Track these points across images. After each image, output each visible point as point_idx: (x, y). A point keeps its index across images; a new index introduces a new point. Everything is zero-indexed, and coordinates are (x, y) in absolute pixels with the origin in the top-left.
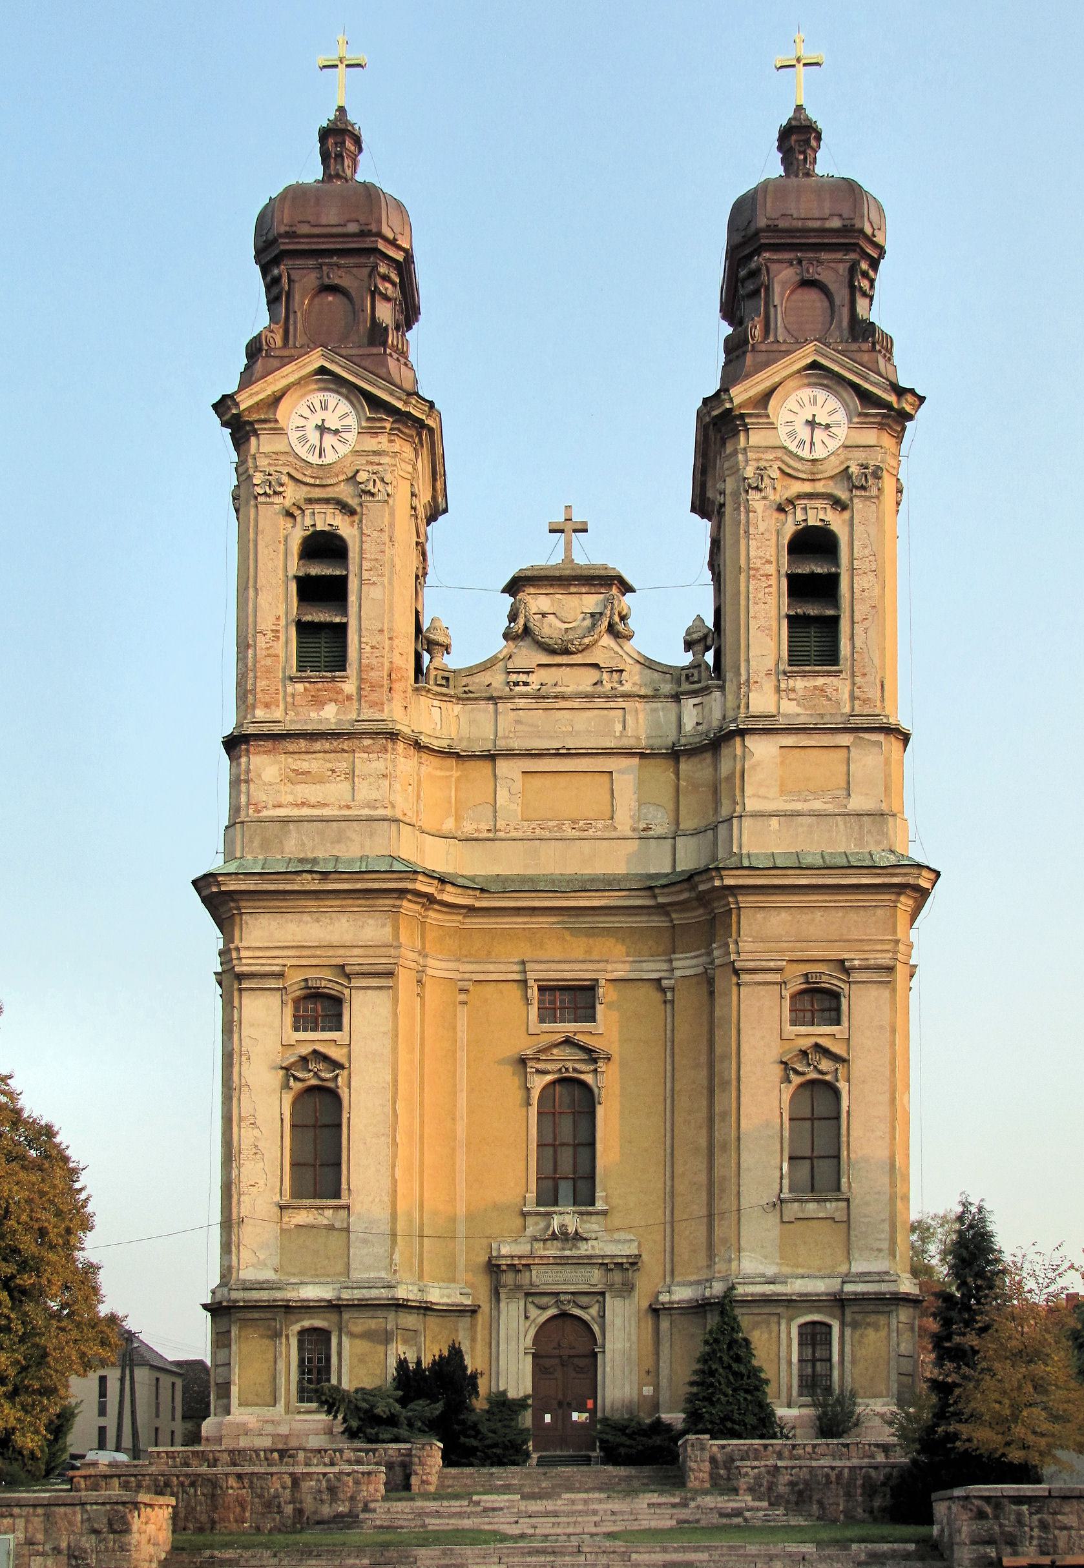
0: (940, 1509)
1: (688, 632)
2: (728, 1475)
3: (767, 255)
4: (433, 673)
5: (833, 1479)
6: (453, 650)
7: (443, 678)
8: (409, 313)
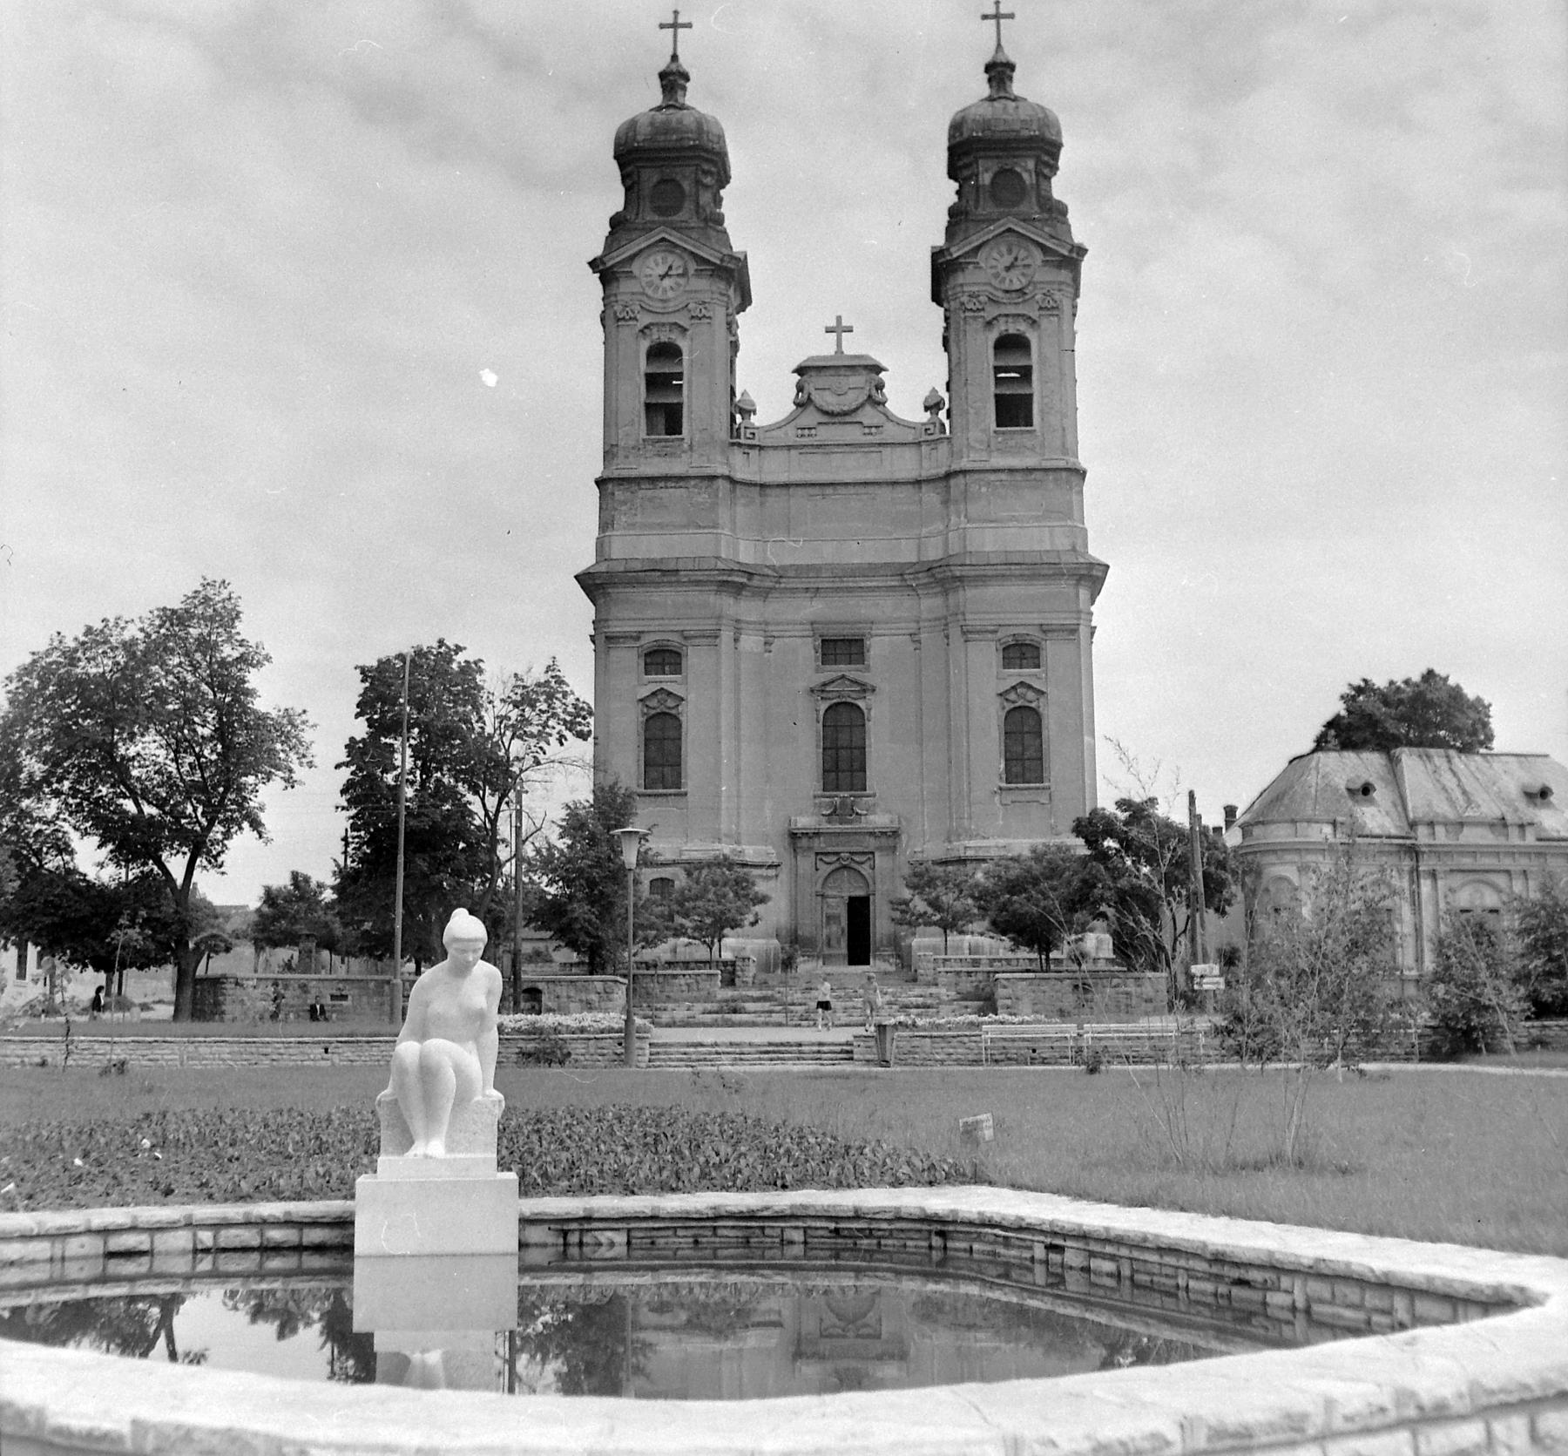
1: (926, 399)
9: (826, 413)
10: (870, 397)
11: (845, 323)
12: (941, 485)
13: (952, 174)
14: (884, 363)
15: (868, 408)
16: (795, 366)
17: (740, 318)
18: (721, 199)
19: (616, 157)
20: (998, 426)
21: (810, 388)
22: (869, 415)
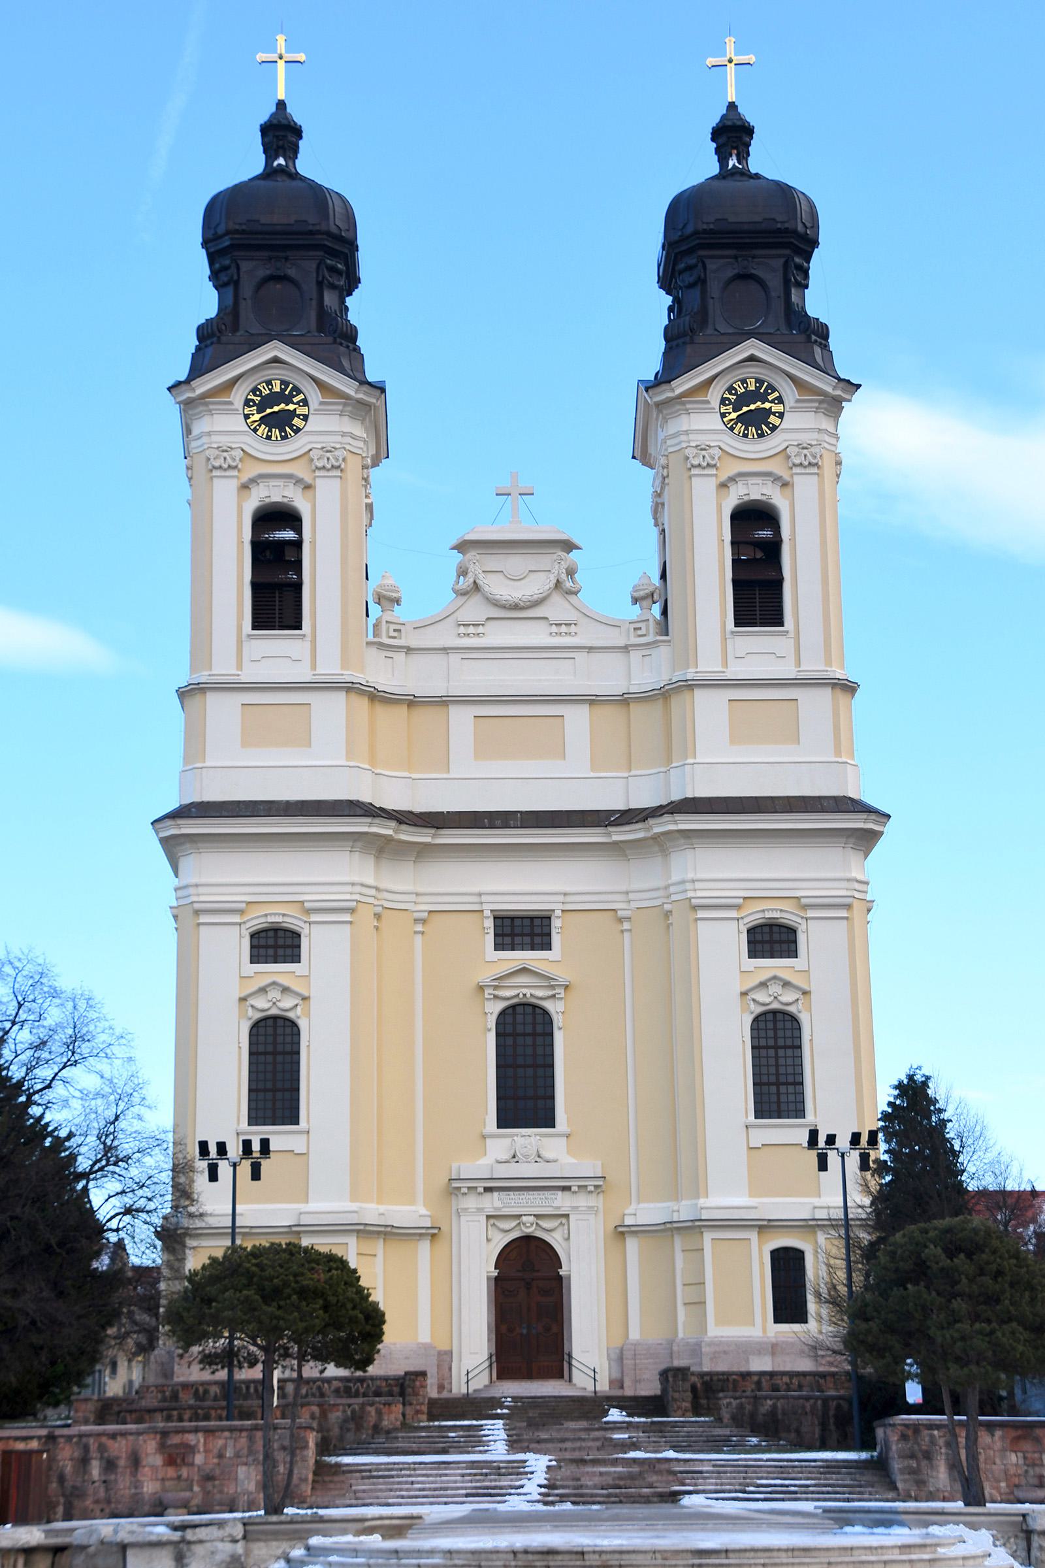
0: (880, 1433)
1: (635, 589)
2: (708, 1405)
3: (702, 253)
5: (808, 1409)
6: (403, 603)
7: (395, 630)
9: (497, 604)
10: (558, 584)
11: (524, 484)
12: (658, 706)
13: (667, 282)
14: (576, 540)
15: (557, 598)
16: (454, 541)
18: (347, 308)
19: (206, 243)
21: (475, 570)
22: (557, 609)
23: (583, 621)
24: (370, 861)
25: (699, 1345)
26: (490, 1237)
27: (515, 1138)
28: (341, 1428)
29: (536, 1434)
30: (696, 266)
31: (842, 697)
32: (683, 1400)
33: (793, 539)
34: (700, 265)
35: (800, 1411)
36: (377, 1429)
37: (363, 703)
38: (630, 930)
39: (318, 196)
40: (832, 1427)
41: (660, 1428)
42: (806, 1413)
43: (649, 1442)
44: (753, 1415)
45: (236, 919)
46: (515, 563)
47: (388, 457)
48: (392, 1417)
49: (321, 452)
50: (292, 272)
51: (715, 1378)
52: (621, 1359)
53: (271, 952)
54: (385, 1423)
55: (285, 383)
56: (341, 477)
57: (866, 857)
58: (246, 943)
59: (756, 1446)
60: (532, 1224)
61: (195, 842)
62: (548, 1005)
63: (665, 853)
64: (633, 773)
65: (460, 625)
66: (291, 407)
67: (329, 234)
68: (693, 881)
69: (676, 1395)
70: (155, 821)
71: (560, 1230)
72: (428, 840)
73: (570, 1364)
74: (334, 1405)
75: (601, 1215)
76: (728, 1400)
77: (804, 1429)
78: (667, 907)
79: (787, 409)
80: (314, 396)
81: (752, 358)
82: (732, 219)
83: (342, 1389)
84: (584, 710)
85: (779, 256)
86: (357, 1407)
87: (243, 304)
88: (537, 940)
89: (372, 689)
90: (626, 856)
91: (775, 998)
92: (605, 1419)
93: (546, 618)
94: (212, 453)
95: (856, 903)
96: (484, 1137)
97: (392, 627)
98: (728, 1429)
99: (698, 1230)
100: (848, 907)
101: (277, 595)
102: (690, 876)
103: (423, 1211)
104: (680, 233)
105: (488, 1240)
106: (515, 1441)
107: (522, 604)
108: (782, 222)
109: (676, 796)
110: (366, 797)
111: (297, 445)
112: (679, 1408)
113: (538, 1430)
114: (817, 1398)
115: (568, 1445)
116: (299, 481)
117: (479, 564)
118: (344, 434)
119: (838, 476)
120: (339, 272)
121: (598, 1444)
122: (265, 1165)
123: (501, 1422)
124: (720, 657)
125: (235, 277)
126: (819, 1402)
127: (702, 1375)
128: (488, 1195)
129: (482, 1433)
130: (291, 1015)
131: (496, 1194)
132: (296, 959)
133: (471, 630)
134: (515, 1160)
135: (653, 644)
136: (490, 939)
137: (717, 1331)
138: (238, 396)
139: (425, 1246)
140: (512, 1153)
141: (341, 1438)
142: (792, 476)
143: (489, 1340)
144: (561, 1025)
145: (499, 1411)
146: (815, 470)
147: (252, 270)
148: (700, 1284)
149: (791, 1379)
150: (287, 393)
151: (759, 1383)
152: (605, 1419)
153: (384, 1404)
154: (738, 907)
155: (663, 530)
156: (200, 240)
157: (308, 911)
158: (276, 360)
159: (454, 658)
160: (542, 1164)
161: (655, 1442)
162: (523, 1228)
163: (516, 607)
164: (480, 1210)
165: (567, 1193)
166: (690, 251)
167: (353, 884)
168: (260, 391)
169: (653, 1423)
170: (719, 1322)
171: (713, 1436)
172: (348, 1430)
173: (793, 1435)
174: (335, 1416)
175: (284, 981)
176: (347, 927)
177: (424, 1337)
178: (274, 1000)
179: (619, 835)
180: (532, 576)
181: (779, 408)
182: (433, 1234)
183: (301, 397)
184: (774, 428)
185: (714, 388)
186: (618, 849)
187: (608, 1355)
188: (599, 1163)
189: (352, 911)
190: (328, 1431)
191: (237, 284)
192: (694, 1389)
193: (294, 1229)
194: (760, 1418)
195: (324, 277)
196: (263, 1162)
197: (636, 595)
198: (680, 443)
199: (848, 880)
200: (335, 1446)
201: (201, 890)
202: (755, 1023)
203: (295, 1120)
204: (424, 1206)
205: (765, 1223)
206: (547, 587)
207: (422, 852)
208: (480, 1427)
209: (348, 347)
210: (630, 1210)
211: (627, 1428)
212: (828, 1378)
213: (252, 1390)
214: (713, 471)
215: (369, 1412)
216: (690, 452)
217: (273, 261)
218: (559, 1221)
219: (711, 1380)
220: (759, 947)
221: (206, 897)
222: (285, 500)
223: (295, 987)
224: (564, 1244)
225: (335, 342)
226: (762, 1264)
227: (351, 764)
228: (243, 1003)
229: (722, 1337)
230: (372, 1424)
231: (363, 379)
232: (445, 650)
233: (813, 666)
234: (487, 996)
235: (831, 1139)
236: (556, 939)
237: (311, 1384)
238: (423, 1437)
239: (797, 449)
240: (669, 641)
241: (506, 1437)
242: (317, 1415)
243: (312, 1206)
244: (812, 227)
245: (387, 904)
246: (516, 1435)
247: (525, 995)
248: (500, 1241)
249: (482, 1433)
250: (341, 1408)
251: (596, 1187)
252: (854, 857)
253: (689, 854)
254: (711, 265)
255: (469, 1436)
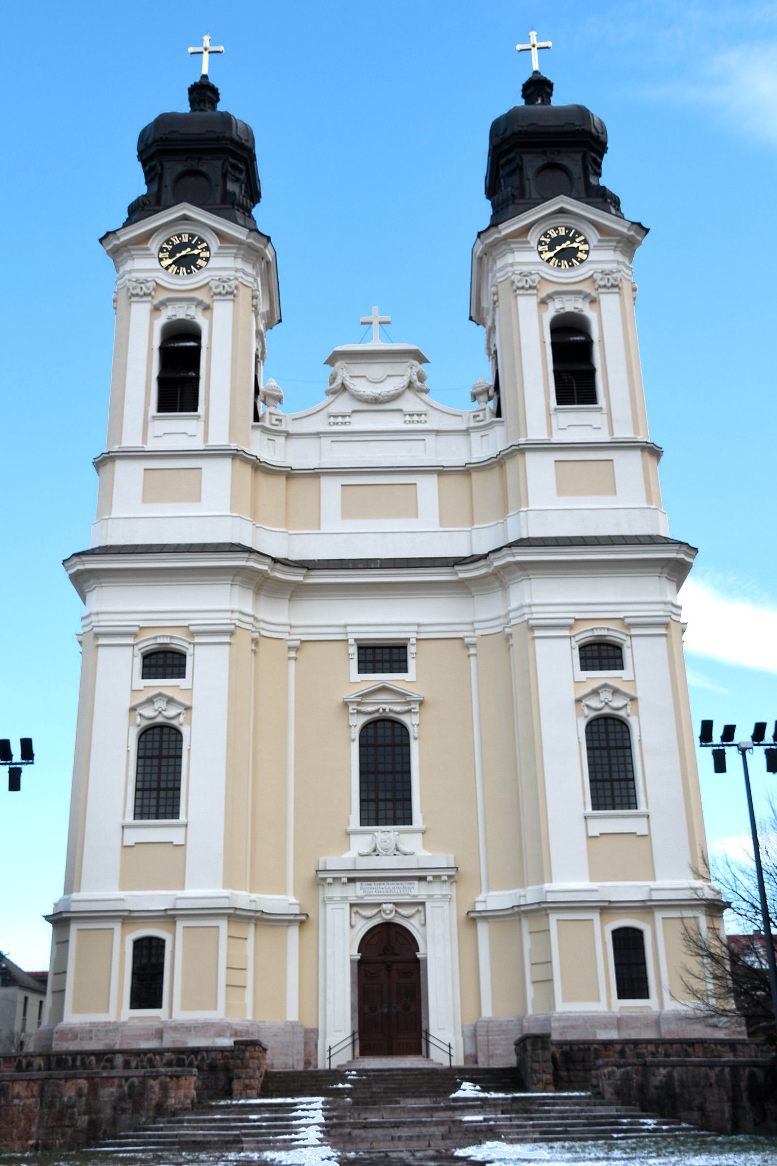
4: (267, 417)
6: (284, 401)
7: (277, 420)
8: (254, 196)
10: (410, 385)
15: (409, 395)
17: (269, 335)
20: (558, 403)
22: (410, 403)
23: (431, 412)
24: (249, 596)
25: (548, 1020)
26: (353, 923)
27: (376, 834)
28: (115, 1108)
29: (363, 1115)
30: (514, 159)
31: (651, 461)
32: (544, 1072)
33: (602, 340)
34: (518, 157)
35: (702, 1083)
36: (160, 1110)
37: (247, 470)
38: (475, 655)
39: (227, 119)
40: (747, 1104)
41: (524, 1107)
42: (711, 1085)
43: (511, 1126)
44: (642, 1088)
45: (130, 641)
46: (376, 370)
47: (280, 321)
48: (181, 1093)
49: (218, 283)
50: (203, 168)
51: (575, 1048)
52: (474, 1035)
53: (160, 670)
54: (172, 1101)
55: (192, 236)
56: (234, 301)
57: (678, 588)
58: (138, 662)
59: (654, 1130)
60: (391, 912)
61: (97, 577)
62: (406, 719)
63: (504, 587)
64: (475, 526)
65: (330, 416)
66: (196, 252)
67: (232, 140)
68: (530, 606)
69: (536, 1066)
70: (64, 561)
71: (417, 916)
72: (300, 579)
73: (427, 1041)
74: (107, 1078)
75: (454, 902)
76: (610, 1069)
77: (710, 1107)
78: (508, 630)
79: (592, 247)
80: (214, 243)
81: (562, 211)
82: (541, 123)
83: (174, 1062)
84: (433, 479)
85: (576, 152)
86: (136, 1080)
87: (164, 190)
88: (396, 665)
89: (255, 458)
90: (471, 593)
91: (606, 703)
92: (453, 1095)
93: (401, 410)
94: (131, 285)
95: (672, 624)
96: (348, 834)
97: (274, 417)
98: (614, 1108)
99: (544, 912)
100: (666, 625)
101: (179, 389)
102: (527, 601)
103: (293, 900)
104: (501, 137)
105: (352, 926)
106: (334, 1126)
107: (381, 398)
108: (580, 126)
109: (511, 539)
110: (248, 543)
111: (199, 278)
112: (539, 1080)
113: (366, 1110)
114: (724, 1065)
115: (404, 1132)
116: (199, 303)
117: (345, 371)
118: (237, 270)
119: (634, 299)
120: (240, 171)
121: (444, 1129)
122: (27, 772)
123: (322, 1099)
124: (546, 431)
125: (159, 171)
126: (727, 1070)
127: (561, 1044)
128: (352, 885)
129: (294, 1114)
130: (175, 722)
131: (358, 884)
132: (182, 675)
133: (340, 419)
134: (376, 853)
135: (490, 425)
136: (354, 664)
137: (564, 1007)
138: (154, 245)
139: (293, 933)
140: (373, 847)
141: (114, 1122)
142: (598, 295)
143: (352, 1019)
144: (416, 735)
145: (340, 1086)
146: (616, 290)
147: (173, 168)
148: (547, 962)
149: (656, 1048)
150: (193, 242)
151: (622, 1053)
152: (453, 1095)
153: (171, 1077)
154: (570, 627)
155: (496, 352)
156: (137, 153)
157: (193, 634)
158: (185, 218)
159: (325, 441)
160: (401, 857)
161: (519, 1126)
162: (384, 915)
163: (376, 401)
164: (344, 898)
165: (423, 883)
166: (509, 151)
167: (232, 611)
168: (172, 242)
169: (514, 1099)
170: (565, 999)
171: (595, 1117)
172: (123, 1111)
173: (696, 1114)
174: (108, 1093)
175: (169, 693)
176: (227, 647)
177: (292, 1015)
178: (160, 709)
179: (464, 573)
180: (390, 380)
181: (586, 247)
182: (302, 921)
183: (205, 245)
184: (582, 261)
185: (533, 232)
186: (463, 588)
187: (463, 1033)
188: (452, 856)
189: (231, 634)
190: (98, 1112)
191: (161, 176)
192: (554, 1060)
193: (169, 913)
194: (652, 1093)
195: (227, 171)
196: (25, 768)
197: (474, 391)
198: (507, 273)
199: (665, 603)
200: (105, 1131)
201: (101, 617)
202: (589, 727)
203: (175, 815)
204: (294, 895)
205: (606, 904)
206: (402, 385)
207: (296, 592)
208: (291, 1107)
209: (244, 214)
210: (481, 898)
211: (482, 1107)
212: (697, 1046)
213: (78, 1063)
214: (535, 292)
215: (152, 1087)
216: (516, 278)
217: (189, 160)
218: (416, 909)
219: (571, 1049)
220: (589, 662)
221: (106, 622)
222: (188, 318)
223: (178, 698)
224: (421, 929)
225: (233, 208)
226: (604, 943)
227: (234, 515)
228: (133, 713)
229: (570, 1012)
230: (154, 1102)
231: (253, 227)
232: (318, 435)
233: (624, 433)
234: (351, 711)
235: (729, 732)
236: (411, 663)
237: (142, 1056)
238: (215, 1120)
239: (601, 275)
240: (503, 422)
241: (323, 1121)
242: (86, 1091)
243: (189, 892)
244: (602, 133)
245: (264, 633)
246: (336, 1117)
247: (384, 710)
248: (363, 927)
249: (294, 1114)
250: (116, 1081)
251: (450, 877)
252: (670, 587)
253: (525, 584)
254: (526, 158)
255: (276, 1119)
